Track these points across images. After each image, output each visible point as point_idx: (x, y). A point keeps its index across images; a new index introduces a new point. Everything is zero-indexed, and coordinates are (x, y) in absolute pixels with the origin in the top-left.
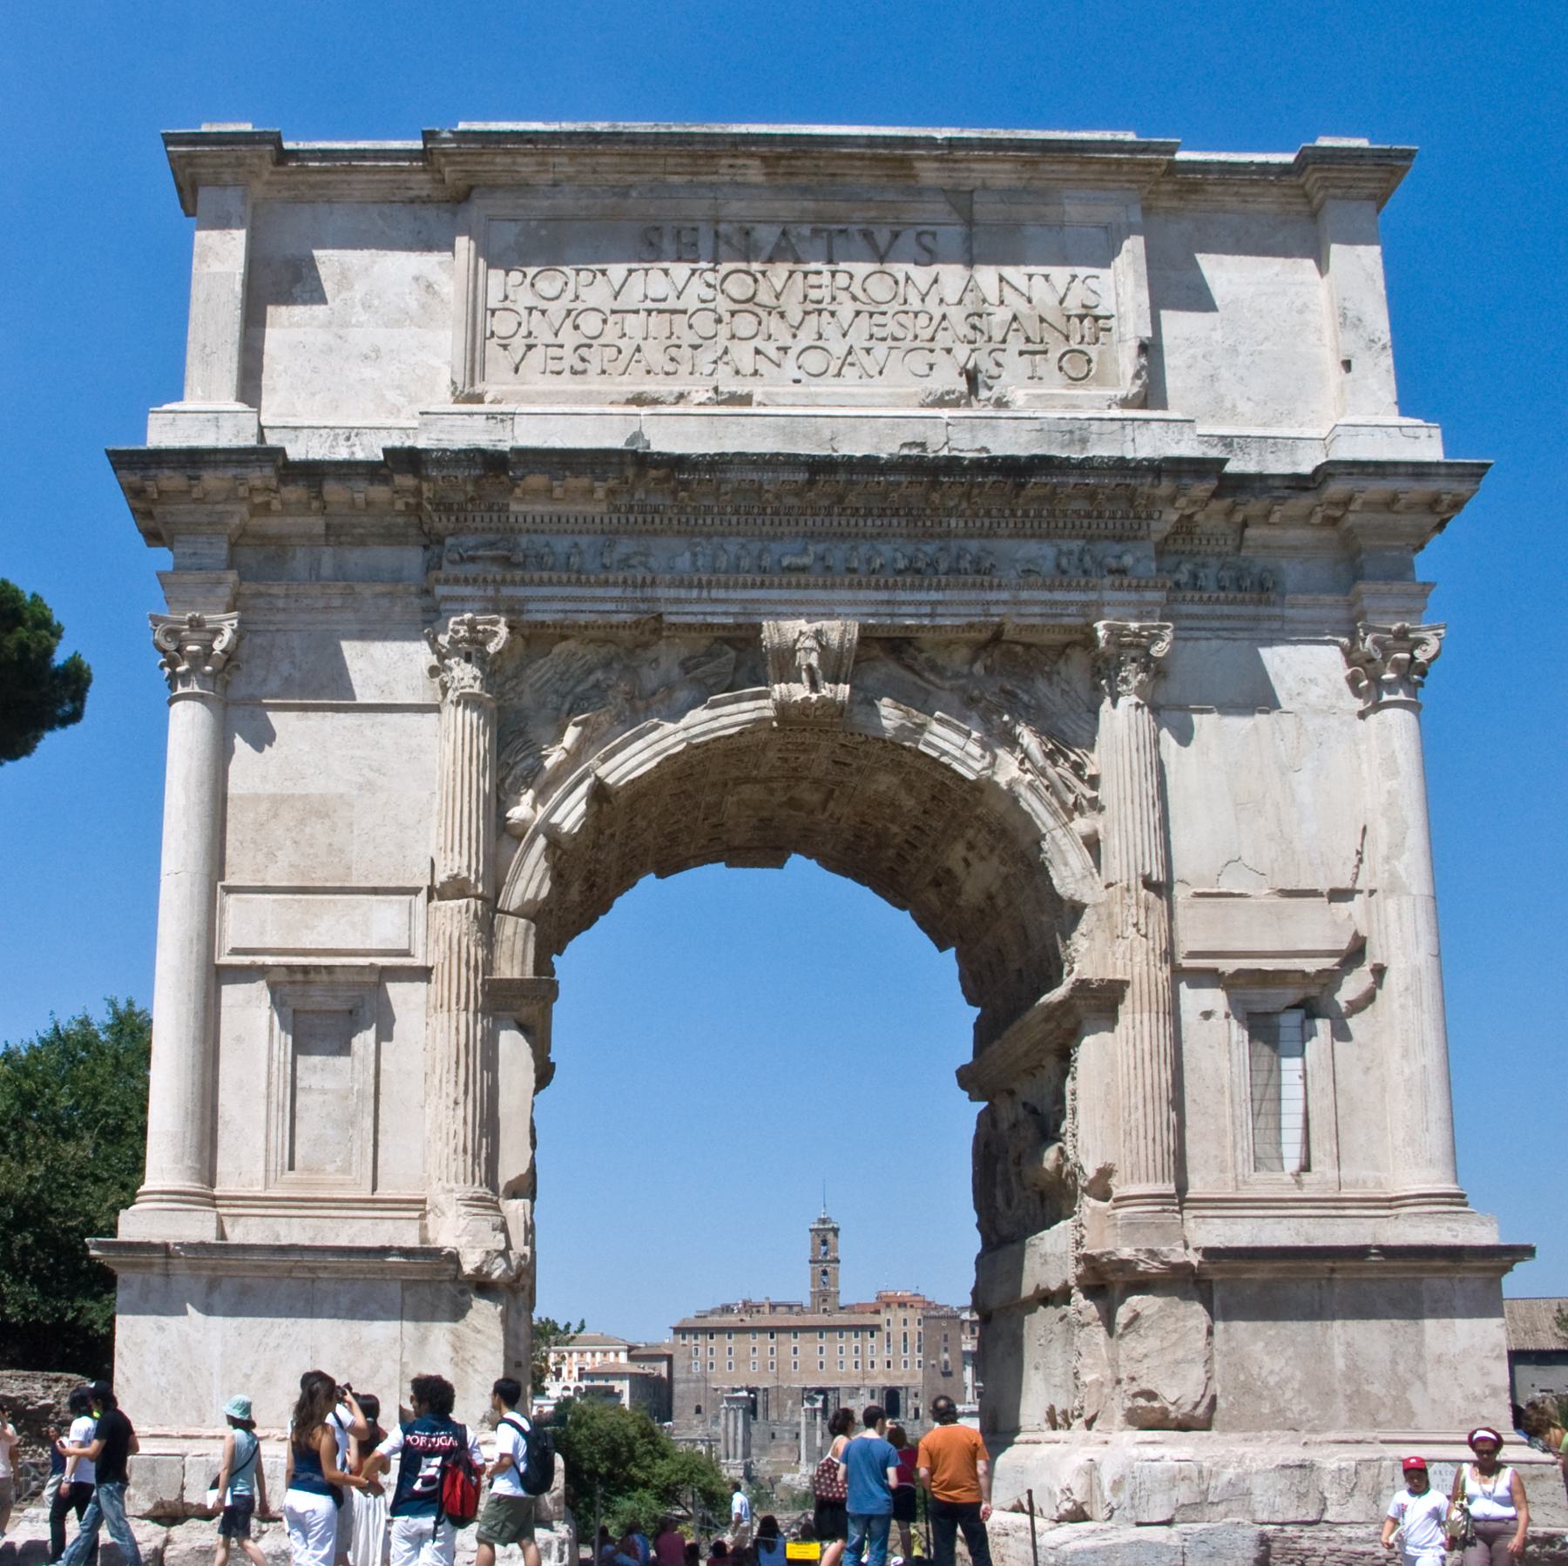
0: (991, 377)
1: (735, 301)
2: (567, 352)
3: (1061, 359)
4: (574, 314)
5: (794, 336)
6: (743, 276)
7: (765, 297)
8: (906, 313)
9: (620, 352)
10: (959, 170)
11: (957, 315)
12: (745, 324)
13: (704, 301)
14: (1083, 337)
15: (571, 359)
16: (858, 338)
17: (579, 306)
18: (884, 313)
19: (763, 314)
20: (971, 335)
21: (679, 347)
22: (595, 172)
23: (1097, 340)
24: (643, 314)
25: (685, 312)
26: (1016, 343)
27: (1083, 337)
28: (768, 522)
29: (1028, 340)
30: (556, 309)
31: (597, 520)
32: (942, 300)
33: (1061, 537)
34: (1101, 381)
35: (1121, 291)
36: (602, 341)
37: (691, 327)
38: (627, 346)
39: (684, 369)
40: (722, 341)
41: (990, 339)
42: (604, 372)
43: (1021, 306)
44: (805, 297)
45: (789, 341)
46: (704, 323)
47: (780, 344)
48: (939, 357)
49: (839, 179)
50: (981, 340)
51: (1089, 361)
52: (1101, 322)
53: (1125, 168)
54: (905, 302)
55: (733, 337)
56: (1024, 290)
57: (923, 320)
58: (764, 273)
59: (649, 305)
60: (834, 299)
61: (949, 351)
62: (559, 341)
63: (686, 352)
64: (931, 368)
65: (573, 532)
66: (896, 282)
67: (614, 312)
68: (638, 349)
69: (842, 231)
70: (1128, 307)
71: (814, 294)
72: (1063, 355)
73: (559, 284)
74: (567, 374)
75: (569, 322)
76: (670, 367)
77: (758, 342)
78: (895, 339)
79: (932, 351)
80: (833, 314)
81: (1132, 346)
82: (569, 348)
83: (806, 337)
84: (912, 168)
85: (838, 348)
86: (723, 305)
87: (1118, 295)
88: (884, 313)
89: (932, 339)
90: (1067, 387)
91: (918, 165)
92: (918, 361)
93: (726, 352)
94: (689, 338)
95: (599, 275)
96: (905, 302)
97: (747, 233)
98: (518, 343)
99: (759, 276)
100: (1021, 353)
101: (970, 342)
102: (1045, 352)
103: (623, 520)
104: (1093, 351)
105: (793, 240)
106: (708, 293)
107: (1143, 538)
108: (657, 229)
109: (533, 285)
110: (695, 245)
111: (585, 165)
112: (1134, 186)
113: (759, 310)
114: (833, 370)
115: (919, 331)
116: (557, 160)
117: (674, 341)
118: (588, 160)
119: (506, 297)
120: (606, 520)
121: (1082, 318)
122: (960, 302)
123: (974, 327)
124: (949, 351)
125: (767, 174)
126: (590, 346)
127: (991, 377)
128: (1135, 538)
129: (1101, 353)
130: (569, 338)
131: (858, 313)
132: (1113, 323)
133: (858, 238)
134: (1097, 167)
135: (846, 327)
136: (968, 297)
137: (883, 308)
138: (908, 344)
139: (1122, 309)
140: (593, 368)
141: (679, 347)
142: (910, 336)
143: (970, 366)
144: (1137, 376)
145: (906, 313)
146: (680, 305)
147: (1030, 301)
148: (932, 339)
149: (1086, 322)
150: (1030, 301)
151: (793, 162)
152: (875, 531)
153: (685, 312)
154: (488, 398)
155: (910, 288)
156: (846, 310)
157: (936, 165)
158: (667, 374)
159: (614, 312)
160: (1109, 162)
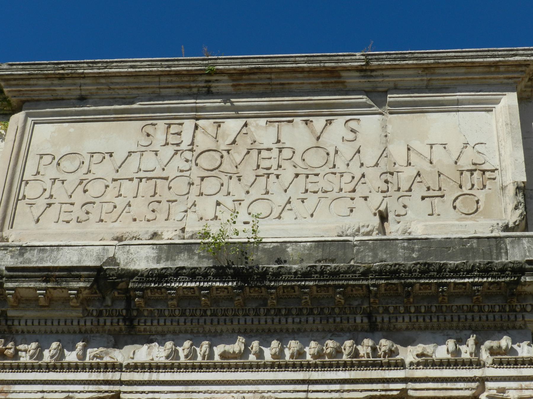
0: (398, 215)
1: (208, 170)
2: (76, 208)
3: (455, 201)
4: (85, 182)
5: (248, 192)
6: (211, 152)
7: (227, 167)
8: (335, 174)
9: (115, 207)
10: (376, 76)
11: (373, 174)
12: (212, 185)
13: (181, 171)
14: (473, 185)
15: (78, 212)
16: (295, 192)
17: (90, 176)
18: (317, 175)
19: (225, 179)
20: (384, 187)
21: (159, 202)
22: (110, 89)
23: (484, 186)
24: (136, 181)
25: (166, 179)
26: (419, 191)
27: (473, 185)
28: (208, 322)
29: (428, 189)
30: (72, 180)
31: (75, 323)
32: (362, 165)
33: (451, 328)
34: (487, 215)
35: (502, 152)
36: (103, 199)
37: (170, 188)
38: (121, 203)
39: (162, 216)
40: (193, 197)
41: (399, 189)
42: (102, 221)
43: (425, 166)
44: (258, 166)
45: (243, 196)
46: (180, 186)
47: (235, 198)
48: (359, 202)
49: (287, 86)
50: (392, 188)
51: (477, 202)
52: (487, 174)
53: (502, 69)
54: (334, 166)
55: (201, 194)
56: (427, 155)
57: (347, 178)
58: (228, 151)
59: (141, 174)
60: (279, 166)
61: (366, 198)
62: (71, 201)
63: (165, 205)
64: (352, 211)
65: (57, 332)
66: (328, 154)
67: (114, 180)
68: (129, 205)
69: (289, 122)
70: (508, 162)
71: (265, 164)
72: (457, 198)
73: (77, 163)
74: (73, 223)
75: (81, 188)
76: (150, 216)
77: (219, 197)
78: (326, 192)
79: (352, 199)
80: (278, 176)
81: (511, 190)
82: (78, 204)
83: (256, 192)
84: (340, 77)
85: (280, 199)
86: (196, 173)
87: (500, 155)
88: (317, 175)
89: (354, 191)
90: (460, 219)
91: (344, 74)
92: (343, 206)
93: (194, 205)
94: (166, 195)
95: (107, 156)
96: (334, 166)
97: (219, 126)
98: (42, 202)
99: (225, 153)
100: (423, 198)
101: (382, 192)
102: (442, 196)
103: (95, 323)
104: (481, 195)
105: (253, 129)
106: (186, 166)
107: (521, 328)
108: (155, 125)
109: (59, 164)
110: (179, 134)
111: (102, 84)
112: (510, 81)
113: (222, 175)
114: (275, 214)
115: (343, 186)
116: (82, 81)
117: (157, 198)
118: (103, 81)
119: (38, 173)
120: (82, 323)
121: (472, 172)
122: (377, 165)
123: (386, 182)
124: (366, 198)
125: (233, 86)
126: (94, 203)
127: (398, 215)
128: (514, 328)
129: (487, 196)
130: (79, 198)
131: (297, 175)
132: (493, 175)
133: (302, 125)
134: (480, 69)
135: (287, 185)
136: (382, 163)
137: (317, 171)
138: (334, 195)
139: (503, 164)
140: (94, 217)
141: (159, 202)
142: (337, 189)
143: (382, 208)
144: (516, 208)
145: (335, 174)
146: (164, 175)
147: (431, 163)
148: (354, 191)
149: (476, 174)
150: (431, 163)
151: (252, 77)
152: (296, 327)
153: (166, 179)
154: (10, 240)
155: (337, 158)
156: (288, 174)
157: (358, 74)
158: (148, 221)
159: (114, 180)
160: (490, 65)
